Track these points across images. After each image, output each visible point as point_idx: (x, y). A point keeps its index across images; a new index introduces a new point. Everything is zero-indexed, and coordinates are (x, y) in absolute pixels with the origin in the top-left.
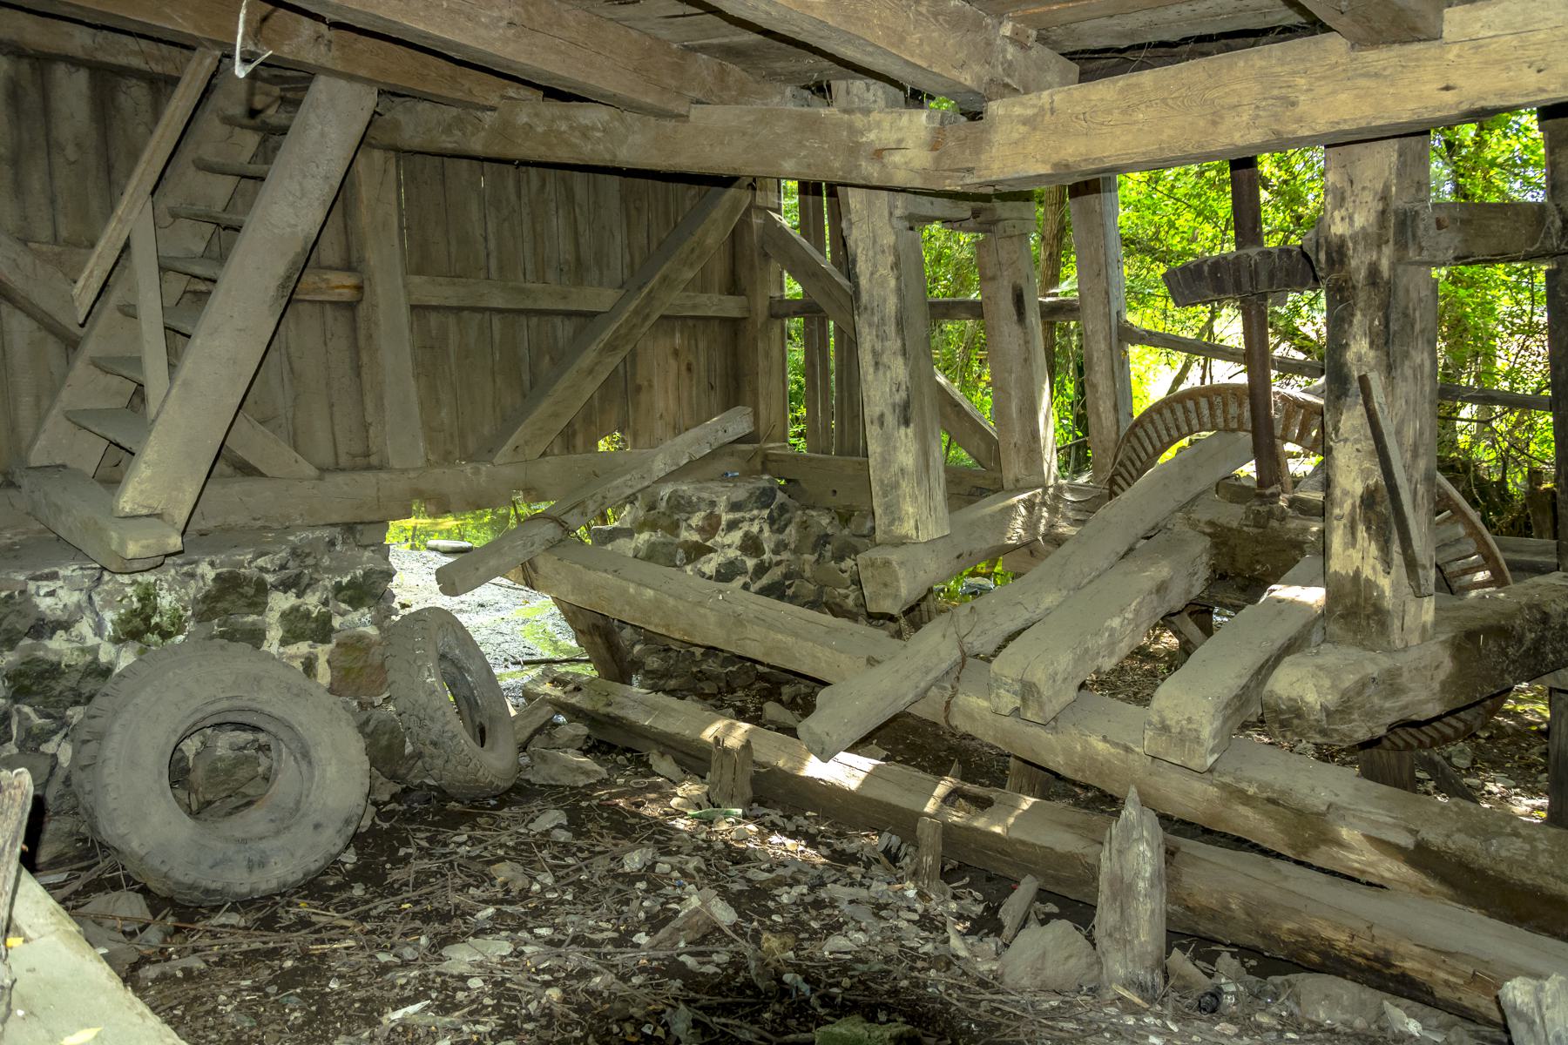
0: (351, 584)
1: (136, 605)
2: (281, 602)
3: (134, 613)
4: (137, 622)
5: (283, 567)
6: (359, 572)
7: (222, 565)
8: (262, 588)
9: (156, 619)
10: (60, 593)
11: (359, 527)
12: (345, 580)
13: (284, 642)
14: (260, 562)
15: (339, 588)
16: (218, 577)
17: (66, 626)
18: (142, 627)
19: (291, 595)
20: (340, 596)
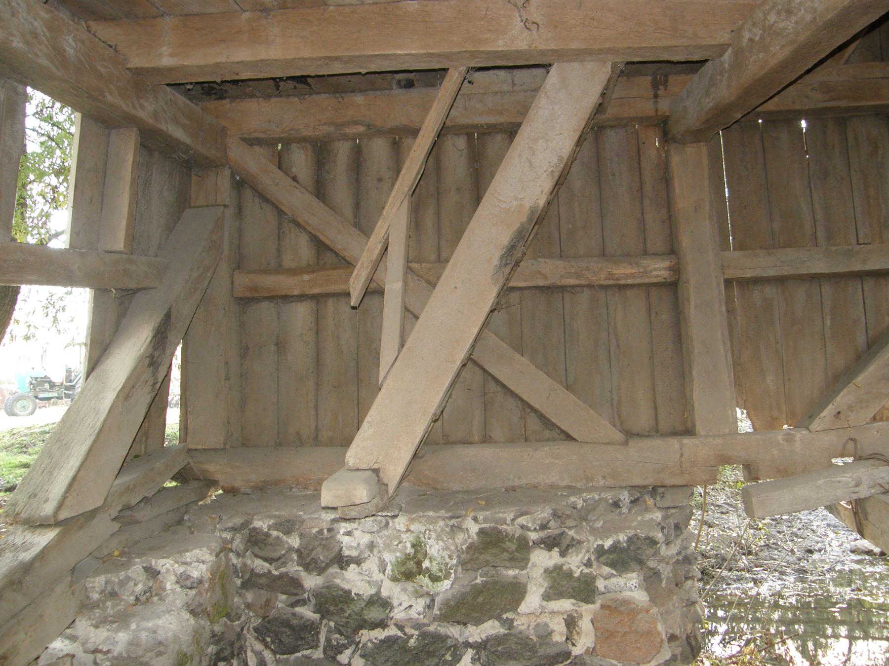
0: (615, 548)
1: (410, 550)
2: (543, 560)
3: (408, 557)
4: (411, 565)
5: (544, 527)
6: (622, 537)
7: (485, 520)
8: (524, 546)
9: (426, 564)
10: (356, 533)
11: (661, 490)
12: (608, 543)
13: (547, 597)
14: (522, 520)
15: (600, 552)
16: (481, 532)
17: (358, 561)
18: (415, 570)
19: (556, 551)
20: (602, 559)
